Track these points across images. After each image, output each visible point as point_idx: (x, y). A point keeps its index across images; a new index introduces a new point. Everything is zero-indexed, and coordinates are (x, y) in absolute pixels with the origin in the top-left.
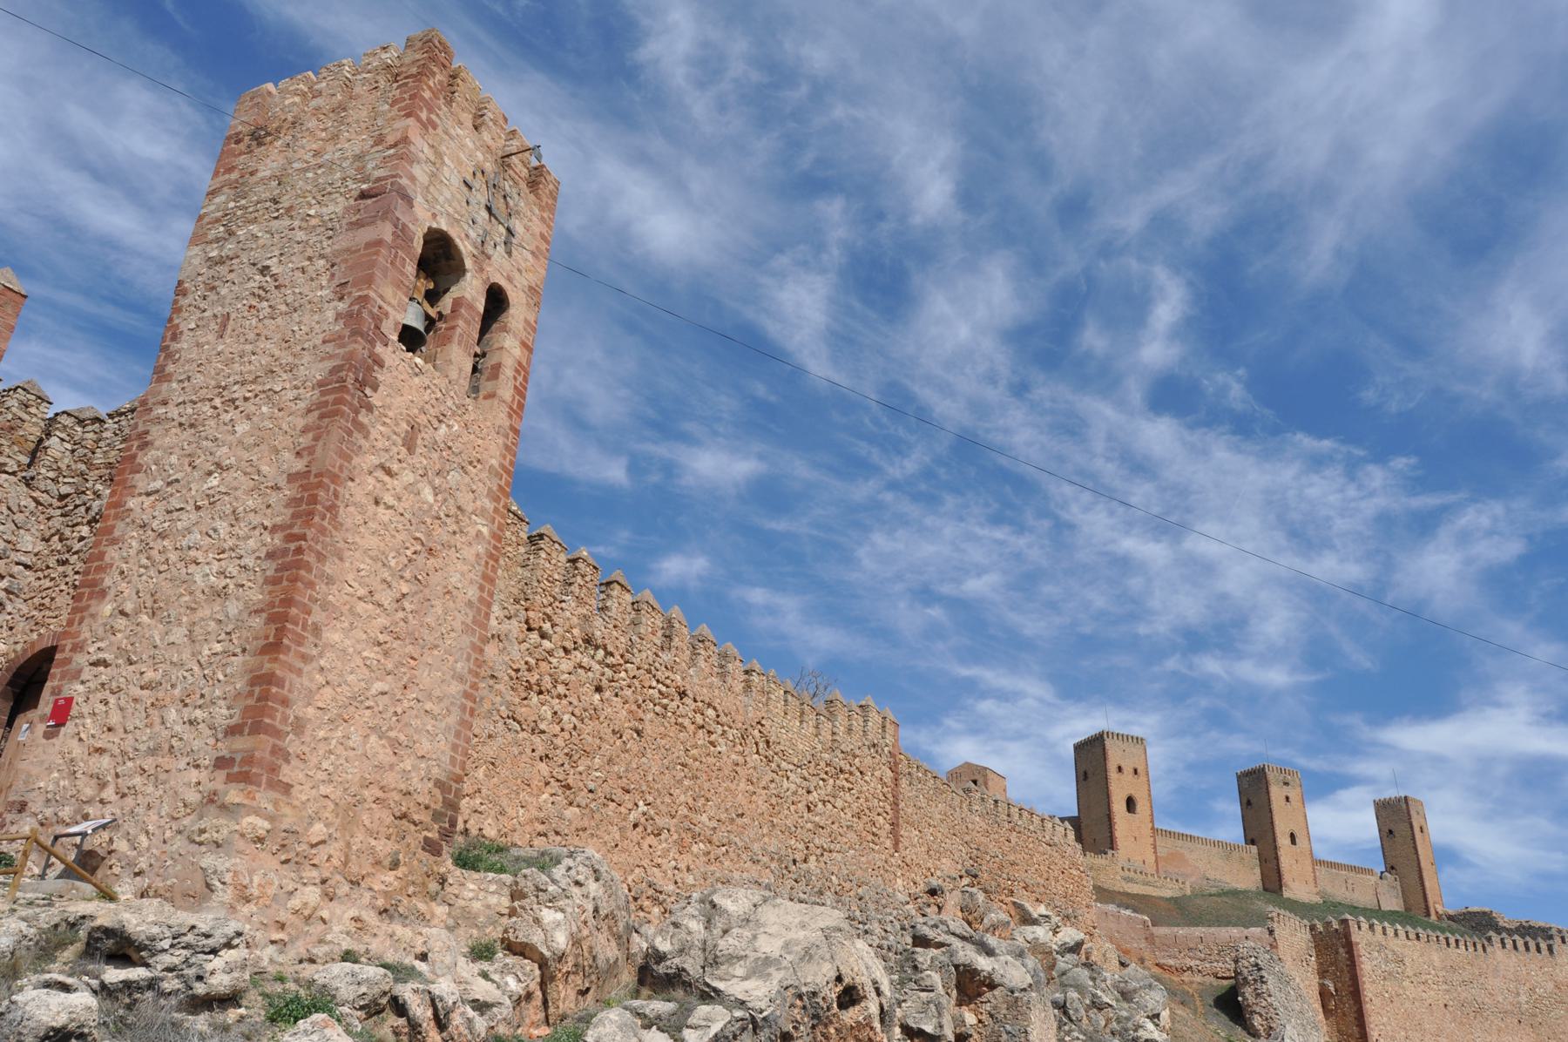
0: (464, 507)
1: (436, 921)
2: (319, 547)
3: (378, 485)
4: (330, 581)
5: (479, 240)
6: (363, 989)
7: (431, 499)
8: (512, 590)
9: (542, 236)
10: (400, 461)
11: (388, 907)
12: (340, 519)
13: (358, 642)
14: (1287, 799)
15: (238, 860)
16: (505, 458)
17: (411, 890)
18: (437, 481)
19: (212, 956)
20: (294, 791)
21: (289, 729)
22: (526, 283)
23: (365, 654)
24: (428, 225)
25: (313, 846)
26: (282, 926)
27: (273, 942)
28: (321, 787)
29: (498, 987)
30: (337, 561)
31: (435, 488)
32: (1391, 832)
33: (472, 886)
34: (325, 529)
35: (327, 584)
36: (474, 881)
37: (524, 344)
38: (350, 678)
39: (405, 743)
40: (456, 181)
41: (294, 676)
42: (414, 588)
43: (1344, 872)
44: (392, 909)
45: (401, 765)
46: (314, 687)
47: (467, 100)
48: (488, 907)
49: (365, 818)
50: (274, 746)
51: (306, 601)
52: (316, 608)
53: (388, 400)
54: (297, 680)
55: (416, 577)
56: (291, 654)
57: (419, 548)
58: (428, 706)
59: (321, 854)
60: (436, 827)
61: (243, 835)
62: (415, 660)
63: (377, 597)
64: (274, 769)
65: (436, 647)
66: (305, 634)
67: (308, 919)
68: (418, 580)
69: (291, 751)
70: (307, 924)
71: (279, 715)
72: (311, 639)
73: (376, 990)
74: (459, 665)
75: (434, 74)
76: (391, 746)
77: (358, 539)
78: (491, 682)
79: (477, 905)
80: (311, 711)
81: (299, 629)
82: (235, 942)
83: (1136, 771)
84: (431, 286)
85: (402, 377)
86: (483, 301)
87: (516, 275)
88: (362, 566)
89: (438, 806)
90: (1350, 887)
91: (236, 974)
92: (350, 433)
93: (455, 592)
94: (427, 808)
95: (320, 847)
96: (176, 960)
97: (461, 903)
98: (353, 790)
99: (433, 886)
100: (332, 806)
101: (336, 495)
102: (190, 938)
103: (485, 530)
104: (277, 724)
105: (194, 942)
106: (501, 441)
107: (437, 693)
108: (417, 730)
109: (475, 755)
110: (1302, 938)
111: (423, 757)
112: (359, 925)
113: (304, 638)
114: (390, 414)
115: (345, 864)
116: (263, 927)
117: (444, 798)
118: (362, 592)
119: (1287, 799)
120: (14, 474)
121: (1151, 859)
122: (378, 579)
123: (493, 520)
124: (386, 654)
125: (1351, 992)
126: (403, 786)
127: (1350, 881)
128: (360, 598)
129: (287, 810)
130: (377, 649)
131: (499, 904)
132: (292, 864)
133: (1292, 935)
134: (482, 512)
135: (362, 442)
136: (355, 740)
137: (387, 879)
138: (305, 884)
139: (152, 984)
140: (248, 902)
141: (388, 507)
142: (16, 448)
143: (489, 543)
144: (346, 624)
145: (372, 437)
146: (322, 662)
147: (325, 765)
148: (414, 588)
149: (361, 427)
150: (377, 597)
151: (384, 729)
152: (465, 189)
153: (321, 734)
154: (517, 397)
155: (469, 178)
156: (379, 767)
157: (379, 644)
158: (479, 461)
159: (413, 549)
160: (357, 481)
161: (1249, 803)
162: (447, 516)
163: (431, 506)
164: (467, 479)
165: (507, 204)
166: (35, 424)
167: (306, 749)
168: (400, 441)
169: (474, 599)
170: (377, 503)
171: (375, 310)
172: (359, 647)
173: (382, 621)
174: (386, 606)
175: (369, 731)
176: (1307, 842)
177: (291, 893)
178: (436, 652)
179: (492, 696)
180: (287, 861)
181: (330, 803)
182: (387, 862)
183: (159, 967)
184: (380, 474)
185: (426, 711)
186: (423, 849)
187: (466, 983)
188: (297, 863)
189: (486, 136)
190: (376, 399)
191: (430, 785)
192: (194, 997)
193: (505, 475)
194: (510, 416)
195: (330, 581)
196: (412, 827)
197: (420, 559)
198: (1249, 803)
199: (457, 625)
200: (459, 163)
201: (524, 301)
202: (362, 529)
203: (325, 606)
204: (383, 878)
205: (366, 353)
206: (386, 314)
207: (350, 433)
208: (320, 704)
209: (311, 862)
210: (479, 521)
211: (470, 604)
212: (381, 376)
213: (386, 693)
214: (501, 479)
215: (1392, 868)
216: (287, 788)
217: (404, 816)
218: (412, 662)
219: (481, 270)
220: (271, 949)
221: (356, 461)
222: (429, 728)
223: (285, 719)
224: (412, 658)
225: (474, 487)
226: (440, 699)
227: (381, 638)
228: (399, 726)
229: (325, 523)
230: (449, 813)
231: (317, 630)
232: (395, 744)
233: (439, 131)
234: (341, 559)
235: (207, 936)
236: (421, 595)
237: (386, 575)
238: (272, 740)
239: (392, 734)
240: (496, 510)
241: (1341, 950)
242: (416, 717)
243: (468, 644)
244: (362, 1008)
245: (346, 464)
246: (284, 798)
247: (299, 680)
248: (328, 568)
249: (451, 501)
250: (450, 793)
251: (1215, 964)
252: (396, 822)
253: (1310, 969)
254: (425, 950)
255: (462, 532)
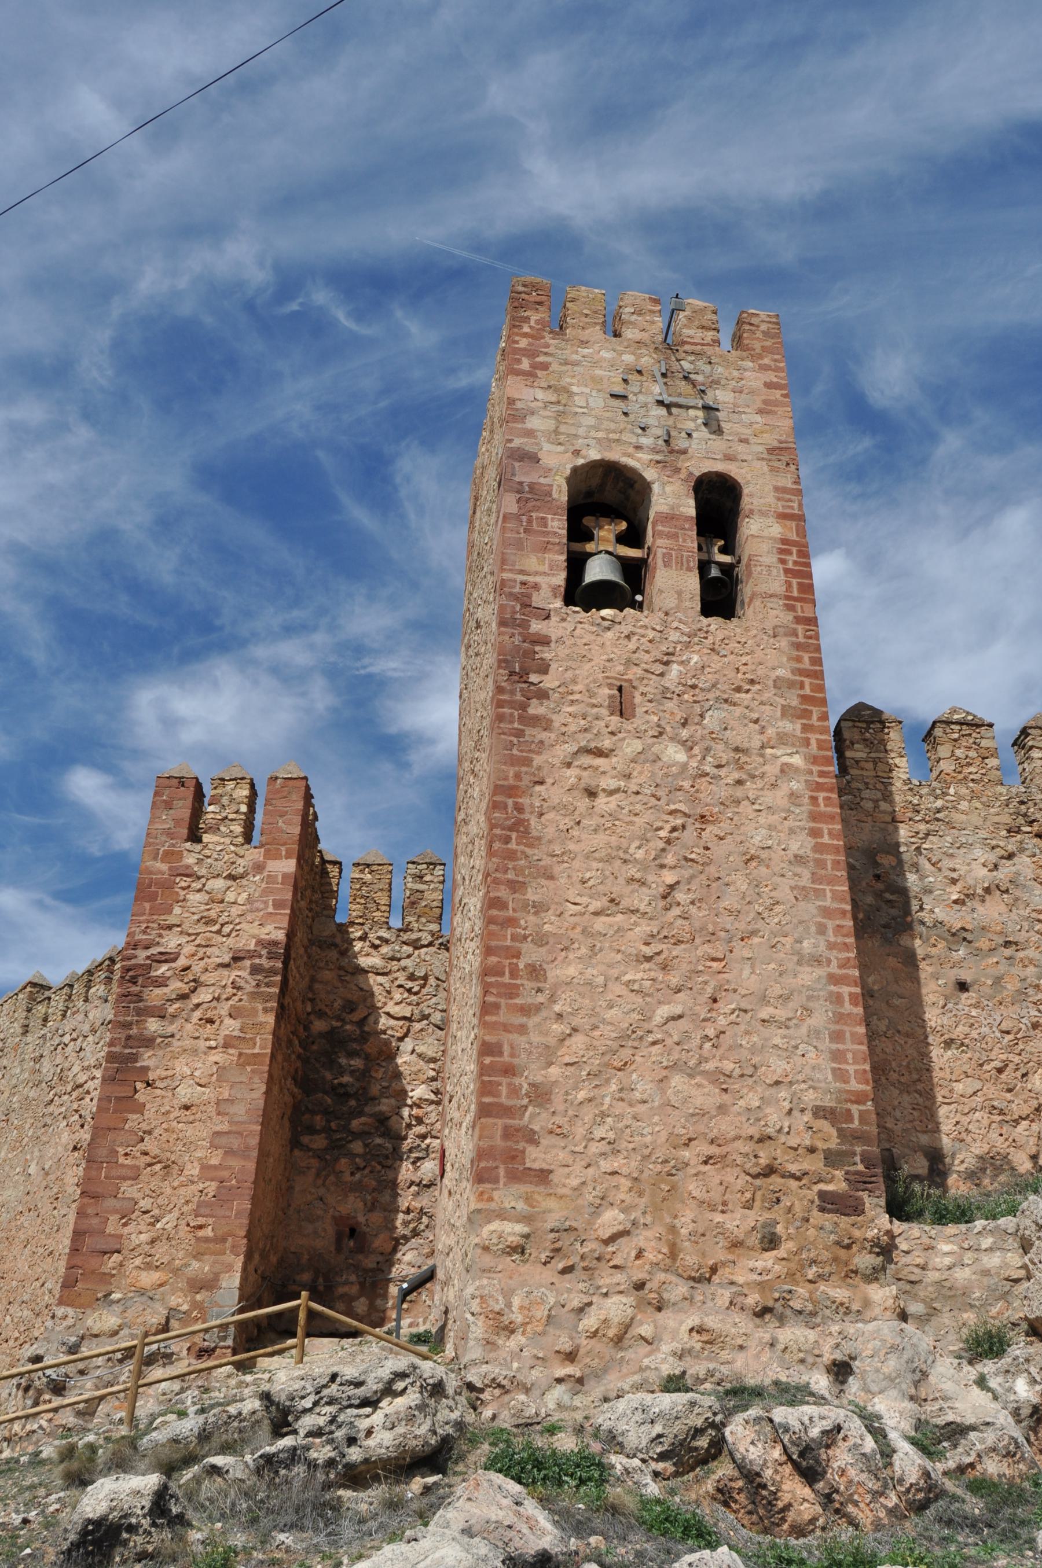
0: (745, 745)
1: (877, 1311)
2: (511, 876)
3: (585, 774)
4: (539, 908)
5: (661, 442)
6: (658, 1429)
7: (681, 757)
8: (997, 819)
9: (769, 385)
10: (612, 733)
11: (770, 1304)
12: (534, 833)
13: (610, 966)
15: (485, 1282)
16: (799, 659)
17: (811, 1272)
18: (685, 733)
19: (368, 1410)
20: (554, 1178)
21: (526, 1101)
22: (761, 449)
23: (627, 977)
24: (569, 467)
25: (607, 1242)
26: (571, 1357)
27: (559, 1381)
28: (602, 1163)
29: (996, 1398)
30: (543, 882)
31: (683, 743)
33: (946, 1248)
34: (515, 852)
35: (536, 913)
36: (949, 1239)
37: (783, 517)
38: (610, 1015)
39: (737, 1072)
40: (598, 401)
41: (515, 1037)
42: (687, 873)
44: (778, 1306)
45: (741, 1103)
46: (552, 1041)
47: (587, 315)
48: (986, 1273)
49: (693, 1187)
50: (506, 1127)
51: (508, 943)
52: (526, 947)
53: (569, 674)
54: (521, 1041)
55: (686, 859)
56: (503, 1010)
57: (679, 822)
58: (765, 1013)
59: (625, 1249)
60: (839, 1174)
61: (486, 1249)
62: (721, 960)
63: (625, 903)
64: (514, 1157)
65: (754, 933)
66: (518, 982)
67: (618, 1341)
68: (692, 860)
69: (536, 1128)
70: (621, 1349)
71: (504, 1090)
72: (529, 985)
73: (678, 1428)
74: (805, 944)
75: (527, 319)
76: (714, 1082)
77: (571, 846)
78: (1008, 952)
79: (962, 1275)
80: (554, 1071)
81: (506, 979)
82: (399, 1385)
84: (624, 525)
85: (584, 641)
86: (692, 502)
87: (741, 448)
88: (588, 875)
89: (834, 1143)
91: (400, 1430)
92: (520, 733)
93: (764, 855)
94: (812, 1150)
95: (622, 1241)
96: (321, 1421)
97: (932, 1276)
98: (660, 1154)
99: (865, 1260)
100: (629, 1184)
101: (519, 808)
102: (333, 1390)
103: (797, 760)
104: (503, 1100)
105: (339, 1395)
106: (784, 643)
107: (777, 990)
108: (753, 1050)
109: (1017, 1059)
111: (777, 1083)
112: (705, 1337)
113: (517, 986)
114: (577, 688)
115: (674, 1253)
116: (539, 1362)
117: (839, 1130)
118: (596, 905)
120: (430, 944)
122: (621, 881)
123: (807, 742)
124: (664, 967)
126: (753, 1131)
128: (596, 914)
129: (552, 1203)
130: (647, 966)
131: (1006, 1265)
132: (578, 1273)
134: (783, 739)
135: (544, 735)
136: (644, 1087)
137: (759, 1264)
138: (606, 1295)
139: (293, 1455)
140: (513, 1332)
141: (611, 793)
142: (424, 920)
143: (811, 772)
144: (584, 951)
145: (556, 724)
146: (557, 1008)
147: (599, 1132)
148: (687, 873)
149: (536, 721)
150: (625, 903)
151: (692, 1063)
152: (617, 403)
153: (582, 1095)
154: (794, 582)
155: (619, 389)
156: (702, 1114)
157: (648, 959)
158: (752, 682)
159: (668, 827)
160: (549, 781)
162: (719, 766)
163: (684, 766)
164: (738, 711)
165: (694, 384)
166: (434, 890)
167: (558, 1120)
168: (604, 712)
169: (807, 851)
170: (592, 794)
171: (517, 589)
172: (614, 972)
173: (645, 928)
174: (643, 907)
175: (664, 1073)
177: (581, 1310)
178: (756, 940)
179: (1016, 970)
180: (567, 1270)
181: (623, 1180)
182: (754, 1240)
183: (302, 1433)
184: (587, 760)
185: (763, 1021)
186: (822, 1210)
187: (945, 1399)
188: (585, 1269)
189: (630, 334)
190: (549, 682)
191: (807, 1117)
192: (350, 1466)
193: (807, 681)
194: (790, 608)
195: (539, 908)
196: (793, 1184)
197: (689, 836)
199: (784, 893)
200: (596, 381)
201: (766, 469)
202: (575, 832)
203: (541, 940)
204: (751, 1264)
205: (517, 639)
206: (536, 587)
207: (520, 733)
208: (567, 1059)
209: (611, 1264)
210: (779, 752)
211: (799, 859)
212: (545, 653)
213: (680, 1017)
214: (802, 687)
216: (543, 1176)
217: (769, 1171)
218: (715, 964)
219: (677, 470)
220: (559, 1392)
221: (538, 760)
222: (777, 1041)
223: (514, 1091)
224: (714, 960)
225: (755, 716)
226: (784, 999)
227: (648, 951)
228: (718, 1053)
229: (513, 846)
230: (858, 1149)
231: (536, 972)
232: (721, 1080)
233: (555, 367)
234: (551, 878)
235: (359, 1384)
236: (703, 877)
237: (633, 871)
238: (500, 1123)
239: (710, 1066)
240: (806, 728)
242: (747, 1033)
243: (815, 911)
244: (662, 1457)
245: (524, 769)
246: (541, 1189)
247: (524, 1038)
248: (531, 895)
249: (720, 747)
250: (852, 1121)
252: (758, 1182)
254: (838, 1356)
255: (753, 777)
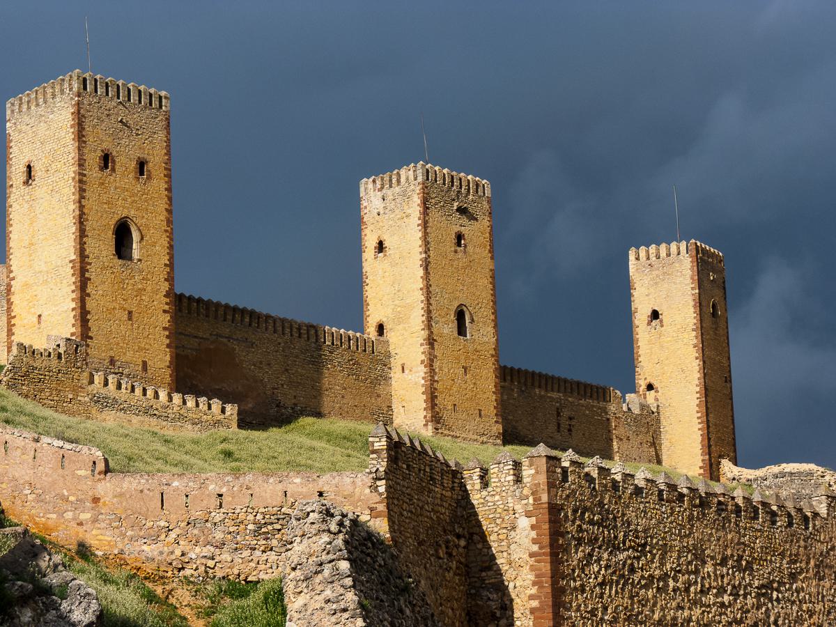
14: (459, 237)
32: (655, 315)
43: (555, 395)
83: (142, 166)
90: (565, 423)
110: (443, 497)
119: (459, 237)
121: (161, 359)
125: (533, 611)
127: (566, 413)
133: (421, 490)
161: (381, 247)
176: (491, 330)
198: (381, 247)
215: (650, 387)
241: (524, 523)
251: (246, 553)
253: (454, 565)
